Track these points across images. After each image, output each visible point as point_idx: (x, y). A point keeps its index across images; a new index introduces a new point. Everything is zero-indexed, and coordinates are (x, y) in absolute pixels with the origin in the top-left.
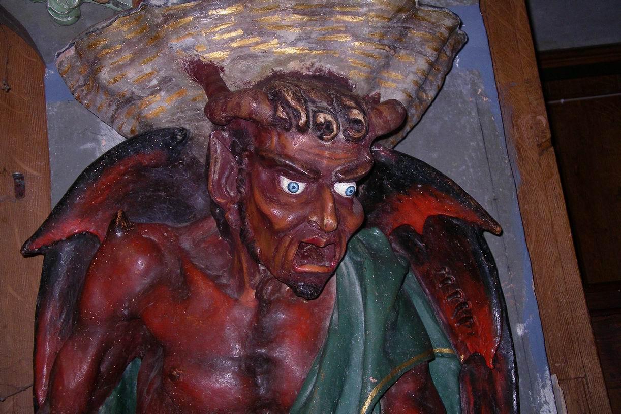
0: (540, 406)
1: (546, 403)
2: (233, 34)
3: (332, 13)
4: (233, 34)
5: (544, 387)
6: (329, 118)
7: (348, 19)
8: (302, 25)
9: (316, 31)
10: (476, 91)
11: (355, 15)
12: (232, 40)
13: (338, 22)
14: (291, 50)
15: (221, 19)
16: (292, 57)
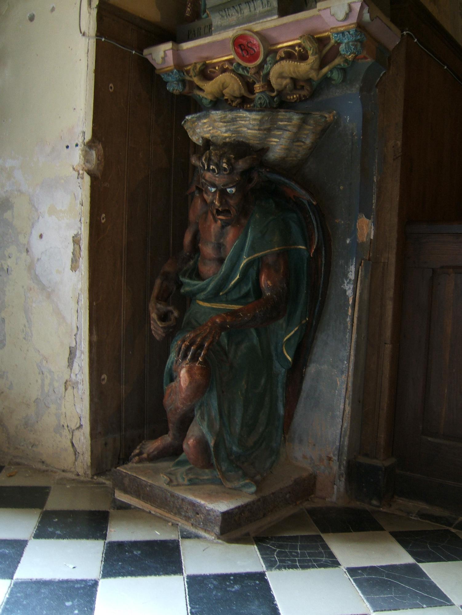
0: (349, 272)
1: (351, 271)
2: (210, 128)
3: (237, 121)
4: (210, 128)
5: (352, 265)
6: (214, 167)
7: (243, 122)
8: (225, 126)
9: (232, 127)
10: (353, 133)
11: (245, 121)
12: (210, 130)
13: (240, 124)
14: (226, 135)
15: (205, 123)
16: (226, 138)
